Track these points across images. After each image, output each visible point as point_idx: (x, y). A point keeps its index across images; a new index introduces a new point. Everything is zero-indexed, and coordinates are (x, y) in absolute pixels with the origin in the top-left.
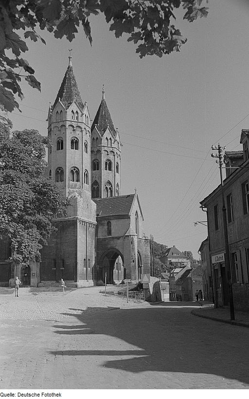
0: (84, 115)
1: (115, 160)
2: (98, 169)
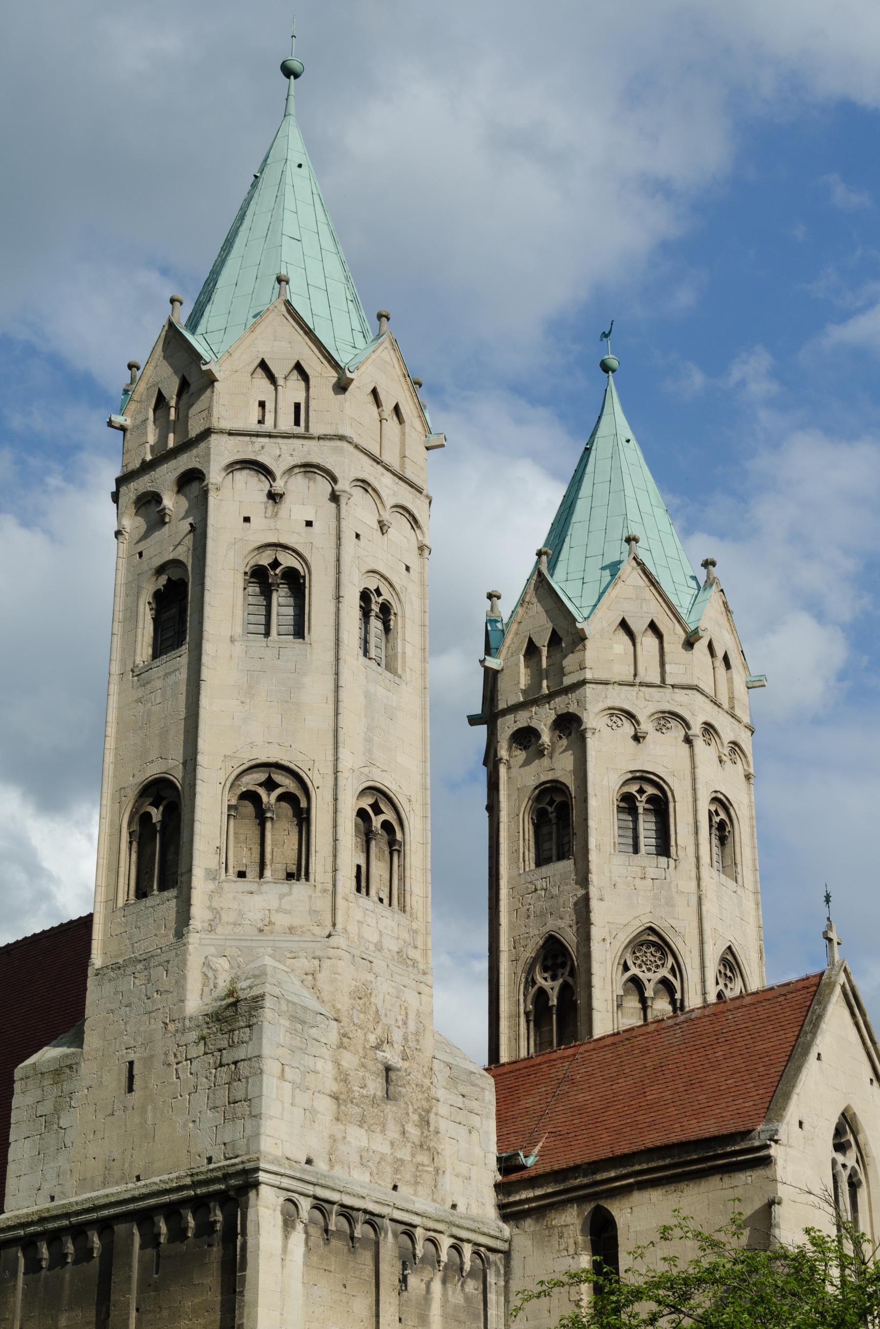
1: (696, 778)
2: (561, 857)
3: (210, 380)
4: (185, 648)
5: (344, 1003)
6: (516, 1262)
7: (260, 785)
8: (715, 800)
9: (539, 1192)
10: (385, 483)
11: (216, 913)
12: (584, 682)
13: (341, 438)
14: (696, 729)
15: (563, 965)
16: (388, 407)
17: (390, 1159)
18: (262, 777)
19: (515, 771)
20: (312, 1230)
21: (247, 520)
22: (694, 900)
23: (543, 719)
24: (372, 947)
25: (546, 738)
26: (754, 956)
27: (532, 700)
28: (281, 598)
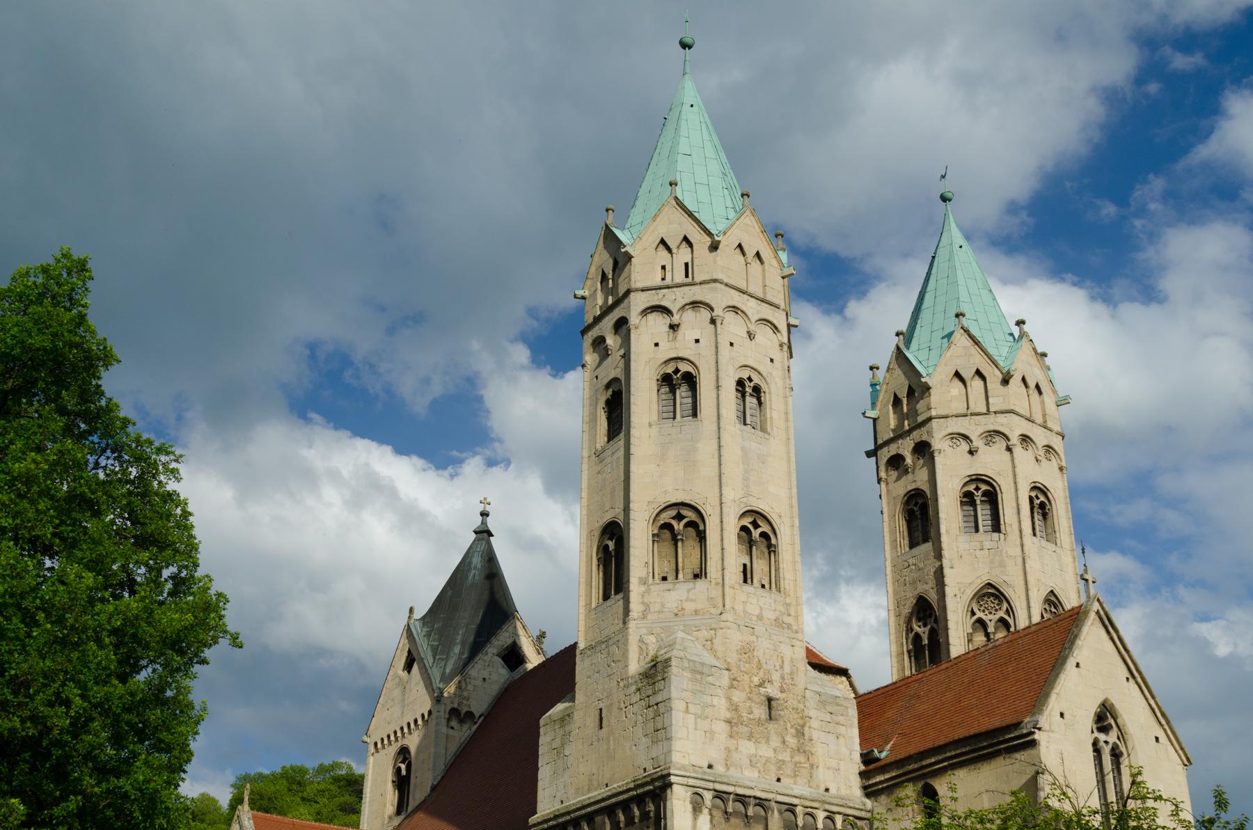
1: (1017, 476)
2: (926, 540)
3: (629, 258)
4: (622, 435)
5: (733, 658)
7: (673, 518)
8: (1034, 488)
9: (887, 776)
10: (750, 306)
11: (647, 606)
13: (715, 281)
14: (1015, 440)
15: (930, 616)
17: (773, 761)
18: (673, 512)
20: (715, 812)
21: (656, 345)
22: (1020, 561)
23: (905, 448)
24: (754, 618)
25: (909, 460)
27: (899, 435)
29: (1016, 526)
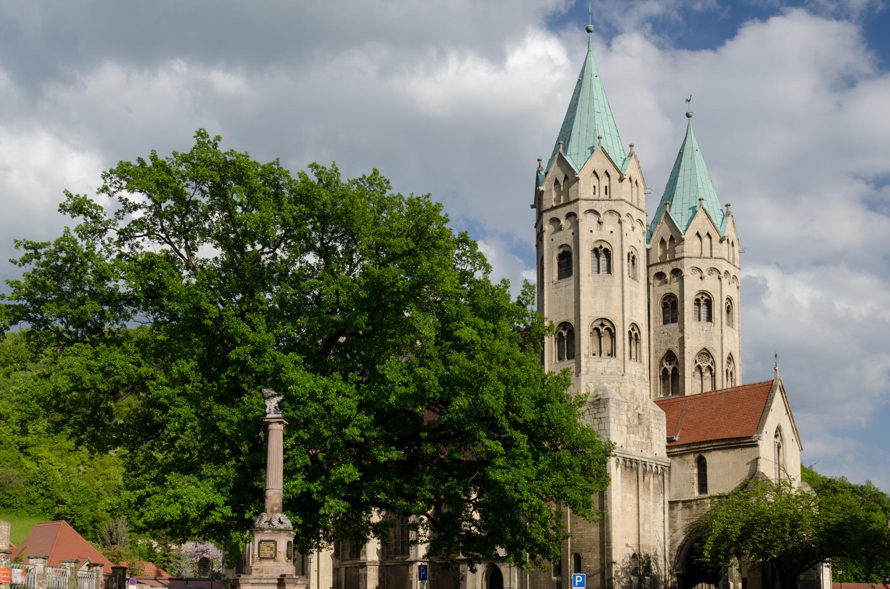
0: (626, 181)
2: (674, 320)
4: (572, 277)
6: (672, 469)
10: (635, 214)
11: (588, 368)
12: (683, 257)
16: (634, 182)
19: (656, 288)
23: (667, 269)
25: (668, 277)
26: (738, 354)
28: (603, 259)
29: (719, 319)
